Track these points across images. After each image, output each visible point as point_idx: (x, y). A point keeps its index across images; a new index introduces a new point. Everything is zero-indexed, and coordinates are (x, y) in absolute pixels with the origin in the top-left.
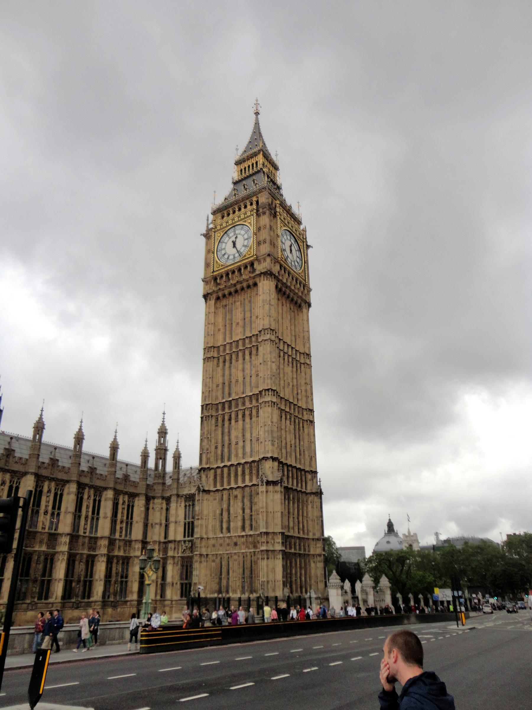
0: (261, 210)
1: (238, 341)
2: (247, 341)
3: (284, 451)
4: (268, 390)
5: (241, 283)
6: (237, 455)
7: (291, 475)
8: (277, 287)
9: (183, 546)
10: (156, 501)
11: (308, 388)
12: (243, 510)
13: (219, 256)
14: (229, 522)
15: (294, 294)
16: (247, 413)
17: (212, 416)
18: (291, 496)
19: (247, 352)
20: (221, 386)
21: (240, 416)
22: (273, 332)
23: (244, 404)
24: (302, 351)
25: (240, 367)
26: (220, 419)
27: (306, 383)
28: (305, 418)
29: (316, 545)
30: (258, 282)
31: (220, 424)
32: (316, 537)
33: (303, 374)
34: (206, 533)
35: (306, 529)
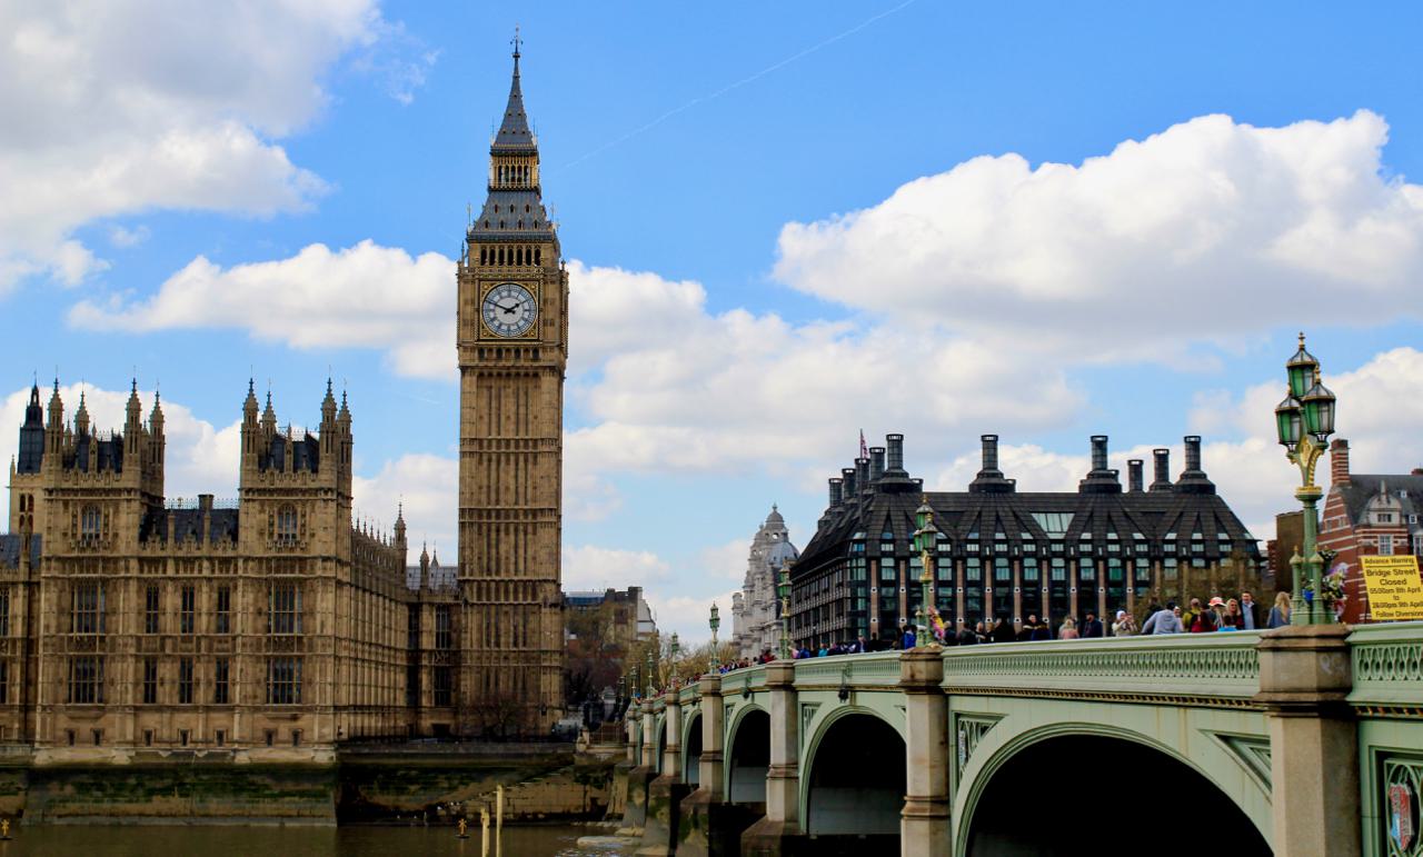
1: (508, 441)
2: (522, 443)
4: (551, 510)
6: (507, 571)
9: (438, 657)
12: (515, 627)
13: (487, 319)
14: (498, 636)
16: (521, 528)
19: (521, 458)
20: (485, 489)
23: (516, 517)
25: (512, 473)
26: (485, 528)
30: (541, 374)
31: (485, 534)
34: (472, 646)
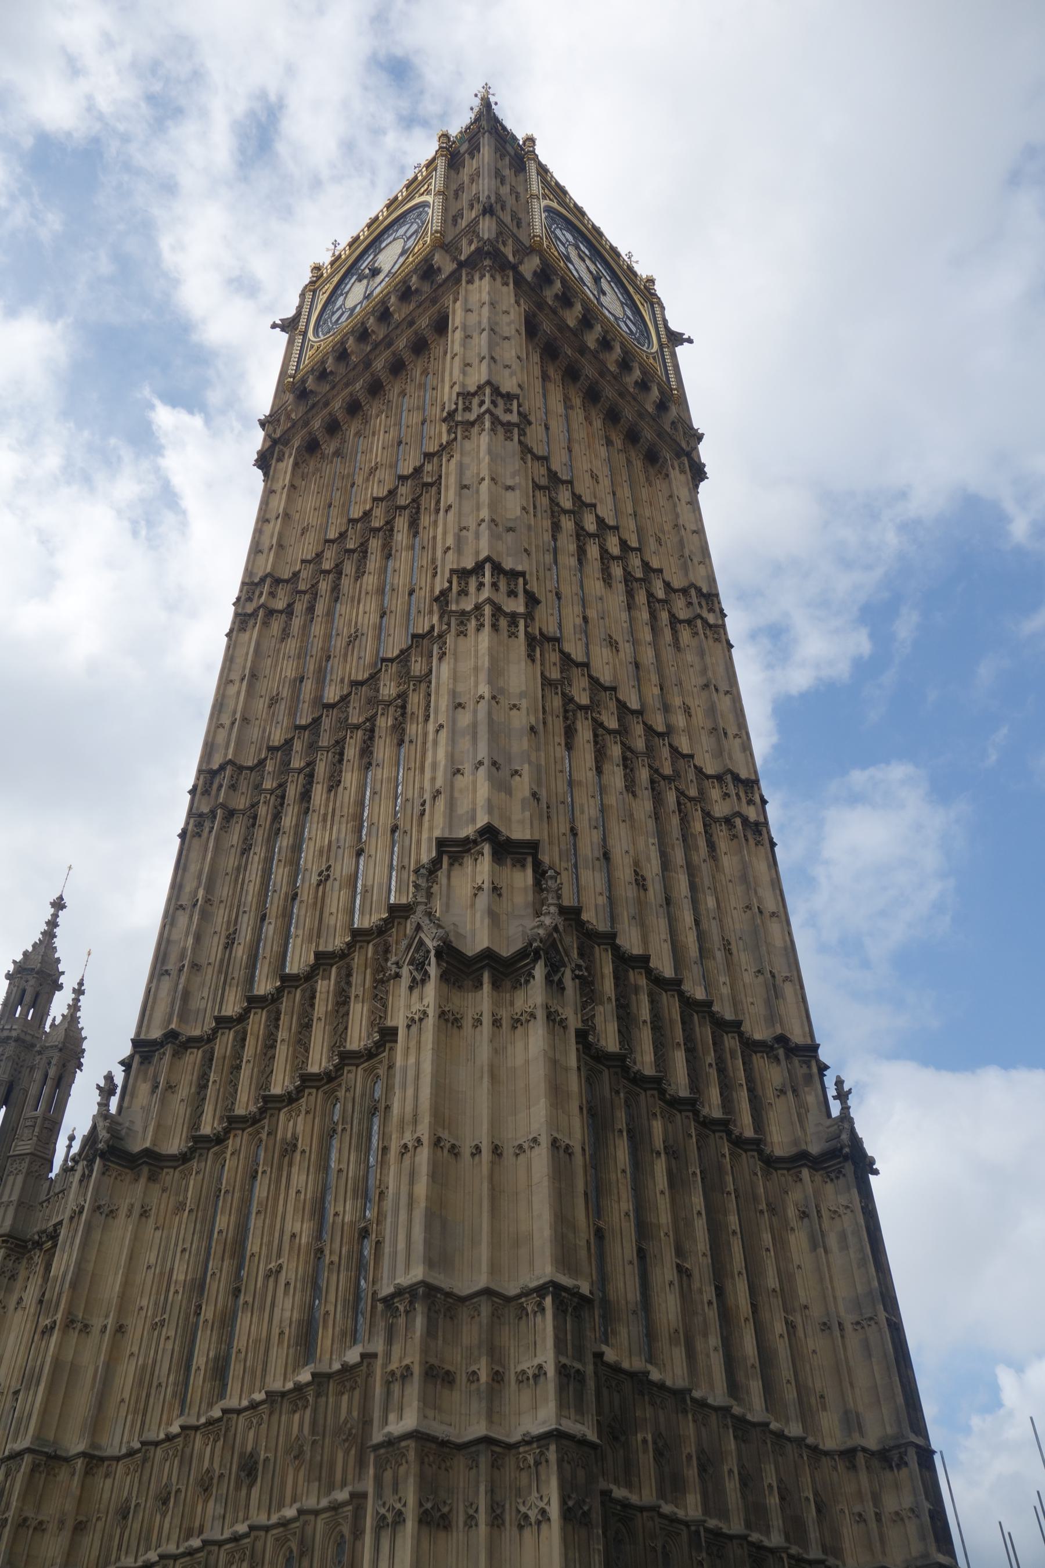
4: (479, 568)
5: (390, 344)
6: (318, 932)
15: (621, 395)
17: (230, 814)
19: (401, 523)
20: (285, 693)
28: (720, 809)
29: (876, 1499)
33: (690, 657)
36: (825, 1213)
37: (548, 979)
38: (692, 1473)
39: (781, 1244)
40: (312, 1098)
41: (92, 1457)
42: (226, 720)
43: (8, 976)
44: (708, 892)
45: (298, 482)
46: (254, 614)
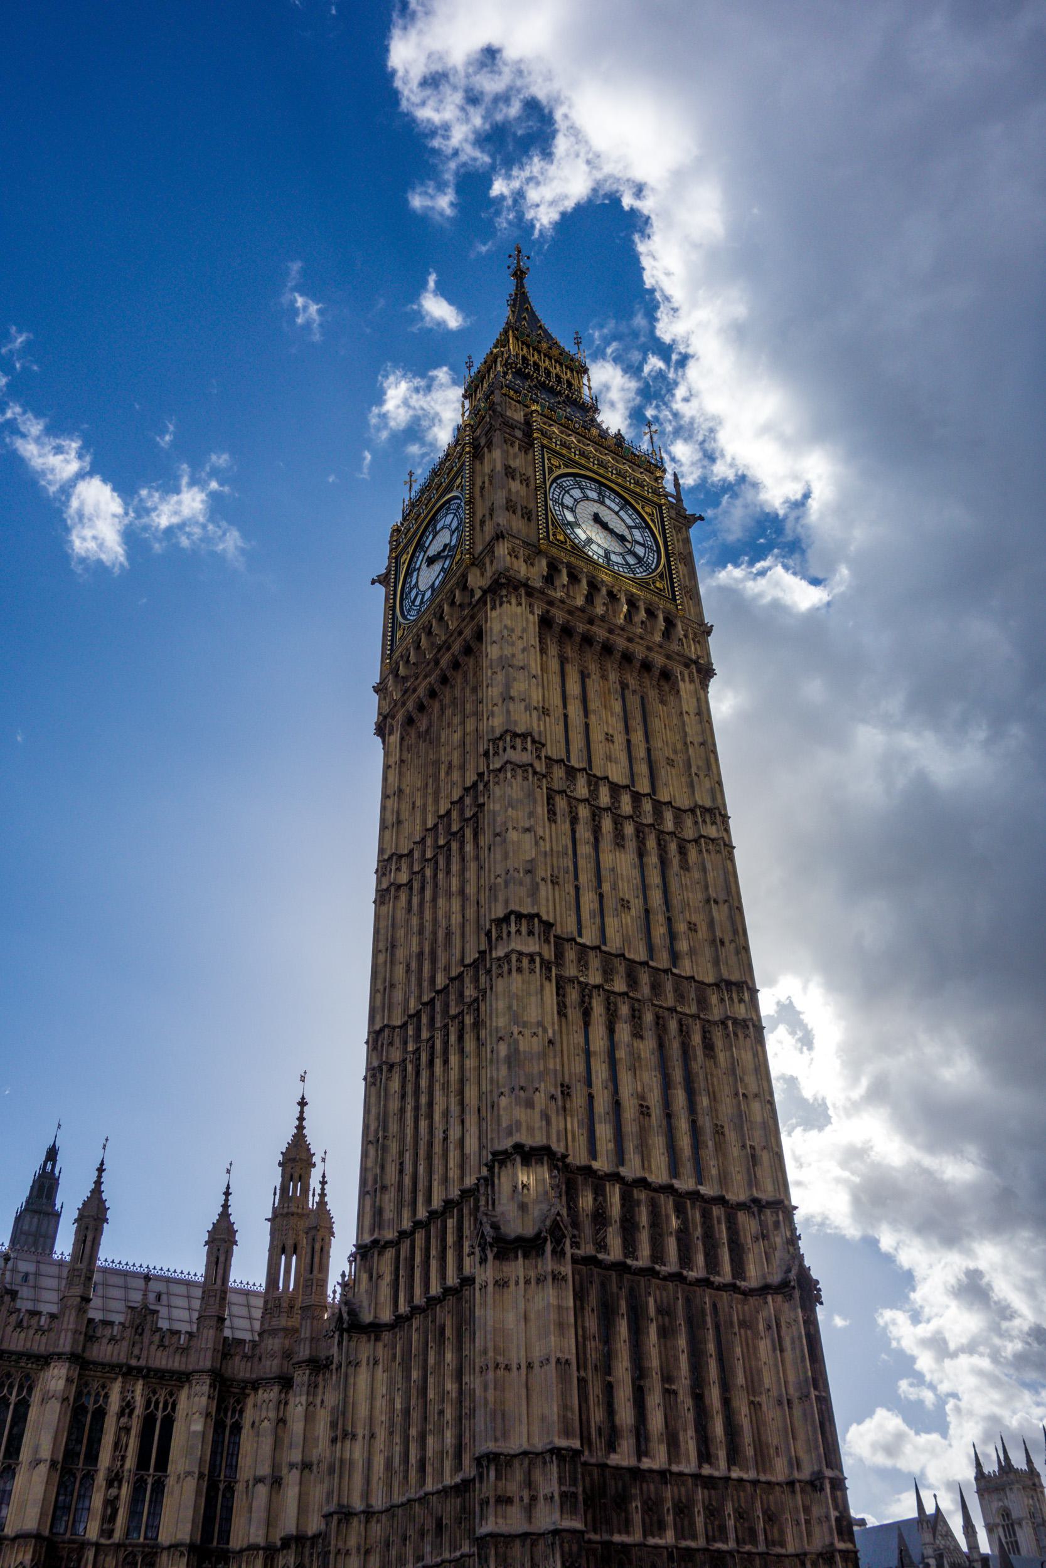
0: (483, 441)
3: (604, 1131)
4: (506, 919)
5: (449, 648)
7: (644, 1219)
8: (545, 622)
10: (262, 1395)
11: (720, 914)
15: (630, 640)
18: (651, 1301)
19: (468, 833)
20: (414, 965)
21: (453, 1038)
22: (524, 742)
24: (684, 802)
25: (455, 882)
27: (708, 901)
29: (807, 1510)
31: (409, 1088)
32: (805, 1474)
33: (696, 874)
35: (747, 1437)
36: (783, 1324)
37: (554, 1252)
38: (669, 1519)
39: (751, 1352)
40: (451, 1301)
41: (368, 1513)
42: (380, 987)
43: (280, 1164)
44: (703, 1093)
45: (407, 756)
46: (388, 890)
